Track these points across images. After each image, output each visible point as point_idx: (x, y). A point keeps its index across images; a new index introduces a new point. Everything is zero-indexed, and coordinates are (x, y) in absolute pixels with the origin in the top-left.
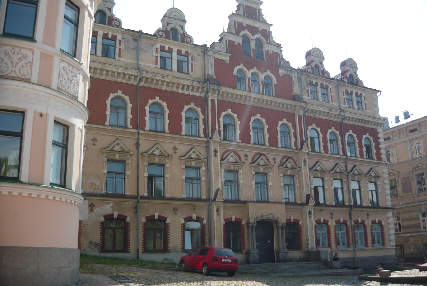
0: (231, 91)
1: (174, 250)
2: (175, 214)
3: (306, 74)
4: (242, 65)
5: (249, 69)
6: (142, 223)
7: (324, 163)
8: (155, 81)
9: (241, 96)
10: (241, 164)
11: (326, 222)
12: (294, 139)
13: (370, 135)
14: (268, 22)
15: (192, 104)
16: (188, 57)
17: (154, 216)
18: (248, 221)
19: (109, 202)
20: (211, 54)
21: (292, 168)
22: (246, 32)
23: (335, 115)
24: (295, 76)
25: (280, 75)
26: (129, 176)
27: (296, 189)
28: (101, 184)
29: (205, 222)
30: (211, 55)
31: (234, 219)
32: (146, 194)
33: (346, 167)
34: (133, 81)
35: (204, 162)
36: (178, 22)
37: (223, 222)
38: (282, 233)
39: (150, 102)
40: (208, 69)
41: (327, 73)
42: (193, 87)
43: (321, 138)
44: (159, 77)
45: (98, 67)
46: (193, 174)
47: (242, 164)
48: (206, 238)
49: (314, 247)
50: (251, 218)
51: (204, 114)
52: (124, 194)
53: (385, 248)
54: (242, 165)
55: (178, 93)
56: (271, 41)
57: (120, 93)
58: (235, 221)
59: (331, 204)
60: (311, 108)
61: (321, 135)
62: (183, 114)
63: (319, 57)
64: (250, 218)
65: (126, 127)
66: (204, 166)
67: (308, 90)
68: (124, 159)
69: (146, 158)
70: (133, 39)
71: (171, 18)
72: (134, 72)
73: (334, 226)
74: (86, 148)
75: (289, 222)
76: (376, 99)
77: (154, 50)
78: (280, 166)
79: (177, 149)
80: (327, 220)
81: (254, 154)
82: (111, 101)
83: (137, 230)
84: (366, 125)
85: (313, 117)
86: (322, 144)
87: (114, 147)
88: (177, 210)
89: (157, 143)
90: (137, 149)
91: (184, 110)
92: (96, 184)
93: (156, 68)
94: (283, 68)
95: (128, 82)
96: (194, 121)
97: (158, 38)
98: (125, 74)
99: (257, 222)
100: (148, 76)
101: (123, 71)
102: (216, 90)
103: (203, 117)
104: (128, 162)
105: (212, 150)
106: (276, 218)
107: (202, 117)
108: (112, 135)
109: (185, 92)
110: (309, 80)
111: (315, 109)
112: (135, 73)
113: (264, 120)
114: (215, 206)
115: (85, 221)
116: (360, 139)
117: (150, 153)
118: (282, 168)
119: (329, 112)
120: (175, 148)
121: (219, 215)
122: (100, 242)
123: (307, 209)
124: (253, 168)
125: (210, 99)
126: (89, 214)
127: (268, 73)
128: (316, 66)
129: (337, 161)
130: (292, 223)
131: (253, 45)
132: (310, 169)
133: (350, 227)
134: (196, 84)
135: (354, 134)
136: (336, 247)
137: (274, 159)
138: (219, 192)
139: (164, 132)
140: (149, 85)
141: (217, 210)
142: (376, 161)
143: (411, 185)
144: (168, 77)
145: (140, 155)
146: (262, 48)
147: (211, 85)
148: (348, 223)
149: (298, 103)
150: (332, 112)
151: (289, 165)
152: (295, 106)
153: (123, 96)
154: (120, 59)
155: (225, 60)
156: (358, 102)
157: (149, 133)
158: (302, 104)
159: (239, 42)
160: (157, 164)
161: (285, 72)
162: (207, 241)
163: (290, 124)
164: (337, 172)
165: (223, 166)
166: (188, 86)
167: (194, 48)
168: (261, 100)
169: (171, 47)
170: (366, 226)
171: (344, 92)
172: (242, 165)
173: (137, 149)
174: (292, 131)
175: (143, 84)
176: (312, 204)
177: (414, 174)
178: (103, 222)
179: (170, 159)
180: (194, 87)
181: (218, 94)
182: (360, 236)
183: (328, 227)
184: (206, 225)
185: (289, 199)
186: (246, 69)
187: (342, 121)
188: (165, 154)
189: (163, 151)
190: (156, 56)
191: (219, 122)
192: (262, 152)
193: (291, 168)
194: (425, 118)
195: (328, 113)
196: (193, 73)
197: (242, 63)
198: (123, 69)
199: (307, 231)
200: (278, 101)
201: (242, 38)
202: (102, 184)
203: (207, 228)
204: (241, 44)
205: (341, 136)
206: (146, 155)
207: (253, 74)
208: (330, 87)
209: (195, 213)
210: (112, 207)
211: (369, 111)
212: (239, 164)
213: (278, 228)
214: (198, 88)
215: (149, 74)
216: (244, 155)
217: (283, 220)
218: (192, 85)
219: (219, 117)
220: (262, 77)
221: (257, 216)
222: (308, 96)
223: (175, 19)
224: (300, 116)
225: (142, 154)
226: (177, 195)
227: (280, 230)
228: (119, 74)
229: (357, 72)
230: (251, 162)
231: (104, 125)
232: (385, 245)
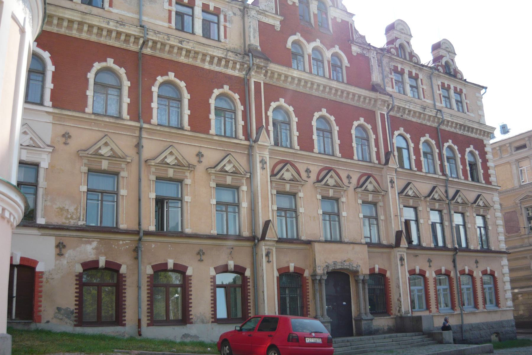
1: (199, 320)
2: (201, 260)
3: (389, 55)
5: (309, 41)
6: (147, 276)
7: (417, 185)
8: (167, 48)
9: (300, 80)
11: (422, 274)
12: (376, 148)
13: (475, 148)
15: (226, 88)
16: (218, 16)
17: (166, 264)
18: (315, 271)
19: (91, 240)
20: (254, 15)
21: (375, 192)
23: (430, 116)
24: (374, 58)
26: (125, 197)
27: (381, 223)
28: (76, 209)
29: (248, 273)
30: (253, 16)
31: (292, 269)
34: (132, 45)
35: (245, 179)
37: (276, 274)
38: (364, 289)
39: (160, 79)
40: (249, 36)
41: (416, 56)
42: (227, 61)
43: (412, 150)
44: (174, 42)
45: (75, 18)
46: (227, 197)
47: (303, 183)
48: (250, 299)
49: (409, 311)
50: (318, 267)
52: (117, 228)
53: (500, 309)
54: (303, 185)
57: (110, 62)
58: (294, 272)
59: (429, 246)
60: (397, 104)
61: (412, 145)
62: (212, 101)
63: (404, 33)
64: (317, 267)
65: (120, 117)
66: (245, 184)
67: (392, 79)
68: (116, 170)
69: (153, 169)
72: (134, 31)
73: (434, 279)
74: (53, 148)
75: (372, 274)
76: (480, 99)
78: (357, 188)
79: (202, 156)
80: (424, 269)
81: (320, 168)
82: (96, 74)
83: (139, 287)
84: (470, 134)
85: (399, 118)
86: (413, 157)
87: (100, 148)
88: (204, 254)
89: (171, 146)
90: (139, 153)
91: (214, 96)
92: (68, 210)
93: (169, 28)
94: (357, 44)
95: (124, 46)
96: (228, 114)
98: (119, 33)
99: (328, 273)
100: (157, 39)
101: (116, 27)
102: (261, 68)
103: (242, 108)
104: (122, 174)
105: (258, 160)
106: (355, 267)
107: (241, 108)
108: (97, 129)
109: (215, 68)
110: (393, 64)
111: (404, 106)
112: (135, 31)
113: (332, 118)
114: (264, 248)
115: (49, 272)
117: (160, 160)
118: (360, 191)
119: (421, 112)
120: (200, 155)
121: (270, 262)
122: (76, 309)
123: (398, 253)
124: (319, 190)
125: (253, 80)
126: (56, 260)
128: (401, 46)
129: (434, 183)
130: (376, 274)
132: (399, 194)
134: (231, 56)
135: (455, 145)
137: (349, 177)
138: (270, 225)
139: (182, 128)
140: (158, 54)
141: (267, 255)
142: (484, 185)
143: (518, 222)
144: (188, 42)
145: (143, 163)
146: (326, 14)
147: (254, 59)
148: (452, 274)
149: (380, 96)
150: (425, 113)
151: (370, 187)
152: (376, 100)
153: (116, 67)
154: (111, 9)
155: (274, 26)
156: (457, 101)
157: (158, 128)
158: (386, 98)
159: (294, 1)
160: (171, 180)
162: (251, 304)
163: (369, 127)
164: (435, 199)
166: (220, 59)
167: (228, 4)
168: (328, 88)
170: (476, 278)
171: (439, 86)
172: (303, 185)
173: (139, 153)
175: (147, 51)
176: (405, 245)
177: (523, 206)
178: (80, 273)
179: (191, 171)
180: (229, 62)
181: (265, 75)
182: (467, 293)
183: (426, 280)
184: (249, 279)
185: (370, 238)
186: (304, 42)
187: (439, 126)
188: (184, 163)
189: (180, 158)
190: (169, 10)
192: (330, 166)
194: (517, 137)
195: (420, 113)
196: (227, 41)
197: (299, 32)
198: (116, 24)
199: (398, 287)
200: (352, 91)
202: (79, 210)
203: (251, 284)
204: (297, 4)
206: (153, 164)
207: (315, 49)
208: (421, 76)
209: (232, 259)
210: (96, 248)
211: (472, 115)
212: (299, 183)
213: (357, 282)
214: (235, 63)
215: (158, 35)
216: (305, 169)
217: (365, 271)
218: (225, 57)
219: (267, 110)
221: (326, 264)
222: (393, 88)
224: (382, 115)
225: (146, 161)
226: (203, 230)
227: (361, 285)
228: (110, 31)
229: (455, 58)
230: (316, 181)
231: (84, 112)
232: (499, 305)
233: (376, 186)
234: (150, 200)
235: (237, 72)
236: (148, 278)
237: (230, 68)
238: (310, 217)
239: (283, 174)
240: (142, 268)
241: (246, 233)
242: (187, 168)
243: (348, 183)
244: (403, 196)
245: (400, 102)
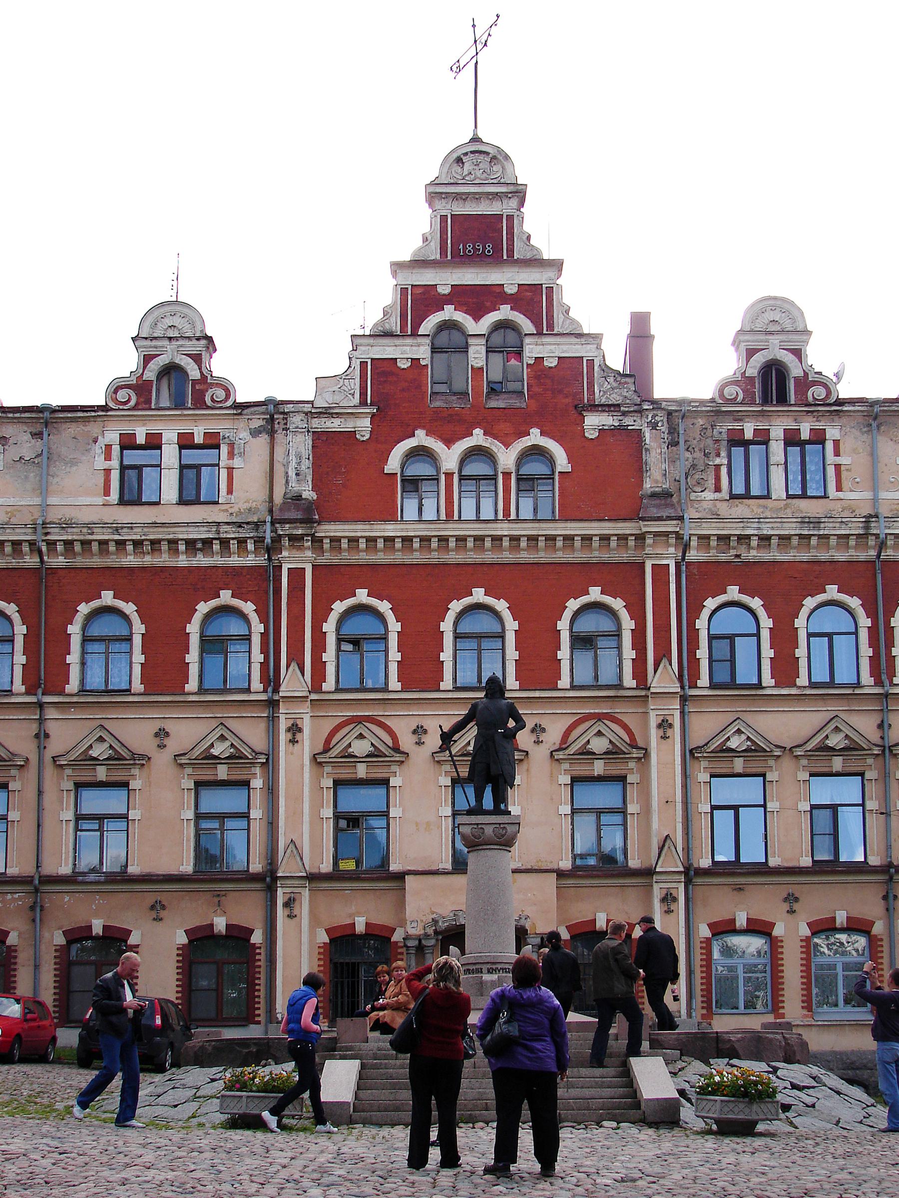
0: (364, 530)
2: (158, 919)
4: (420, 433)
5: (449, 442)
8: (95, 547)
10: (392, 759)
14: (547, 254)
16: (218, 447)
21: (613, 753)
22: (449, 313)
25: (586, 435)
29: (257, 938)
31: (360, 928)
32: (65, 869)
33: (881, 726)
36: (181, 346)
37: (323, 938)
39: (84, 609)
43: (765, 635)
49: (679, 1012)
51: (264, 620)
55: (176, 568)
56: (558, 318)
58: (366, 934)
61: (766, 623)
63: (782, 331)
67: (718, 467)
70: (31, 433)
71: (155, 338)
77: (98, 451)
78: (559, 750)
79: (167, 734)
88: (163, 907)
90: (41, 748)
95: (14, 563)
97: (109, 413)
105: (283, 725)
107: (258, 627)
109: (201, 560)
118: (561, 757)
120: (162, 734)
127: (535, 437)
131: (477, 355)
133: (885, 943)
136: (805, 1012)
137: (538, 729)
146: (519, 354)
147: (278, 525)
150: (821, 532)
152: (641, 538)
161: (607, 420)
162: (262, 994)
163: (617, 604)
165: (328, 769)
167: (236, 417)
172: (403, 762)
173: (41, 748)
184: (260, 948)
187: (879, 556)
193: (605, 753)
197: (423, 428)
201: (427, 341)
205: (871, 613)
206: (66, 763)
208: (832, 433)
214: (242, 542)
219: (320, 617)
220: (507, 458)
223: (170, 338)
224: (660, 571)
226: (165, 865)
233: (613, 740)
234: (62, 824)
235: (251, 557)
236: (56, 950)
237: (234, 553)
238: (417, 824)
239: (350, 745)
240: (47, 935)
241: (256, 867)
242: (132, 762)
243: (535, 742)
244: (705, 755)
245: (722, 525)
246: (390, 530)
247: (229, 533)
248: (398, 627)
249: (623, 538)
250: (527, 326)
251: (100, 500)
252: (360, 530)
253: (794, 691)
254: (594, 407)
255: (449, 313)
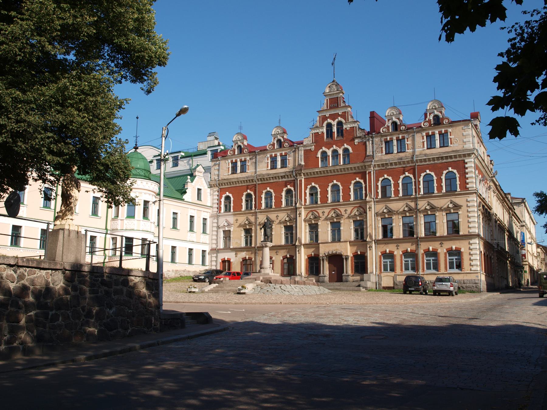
5: (329, 149)
29: (294, 258)
37: (307, 257)
39: (264, 191)
42: (287, 176)
51: (295, 191)
59: (398, 238)
67: (382, 148)
84: (449, 160)
105: (298, 213)
116: (439, 175)
131: (335, 129)
141: (298, 251)
163: (362, 181)
169: (276, 153)
171: (423, 137)
174: (364, 185)
181: (304, 175)
186: (326, 150)
191: (305, 193)
205: (415, 178)
211: (456, 145)
214: (290, 175)
220: (341, 151)
246: (317, 170)
247: (288, 174)
248: (320, 190)
249: (362, 167)
250: (343, 121)
251: (266, 169)
252: (311, 171)
253: (397, 198)
254: (357, 138)
255: (329, 121)
